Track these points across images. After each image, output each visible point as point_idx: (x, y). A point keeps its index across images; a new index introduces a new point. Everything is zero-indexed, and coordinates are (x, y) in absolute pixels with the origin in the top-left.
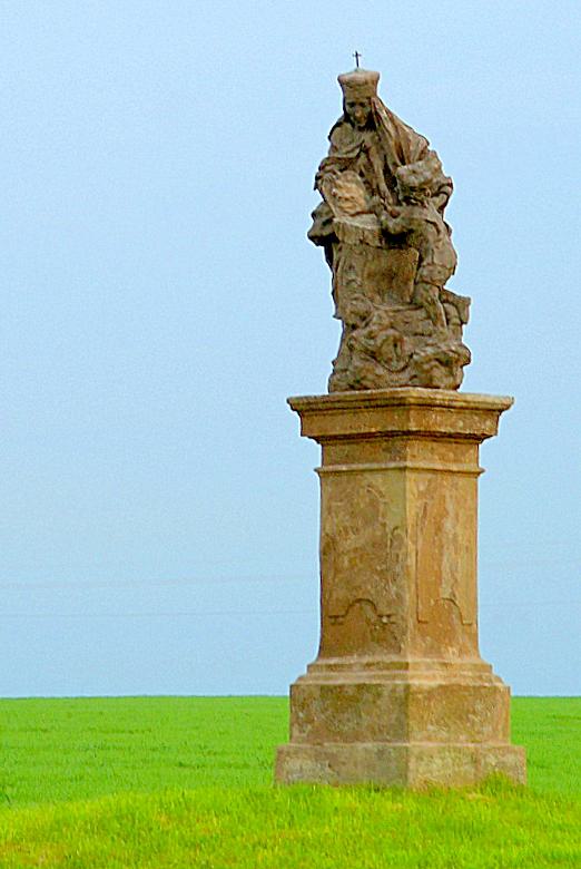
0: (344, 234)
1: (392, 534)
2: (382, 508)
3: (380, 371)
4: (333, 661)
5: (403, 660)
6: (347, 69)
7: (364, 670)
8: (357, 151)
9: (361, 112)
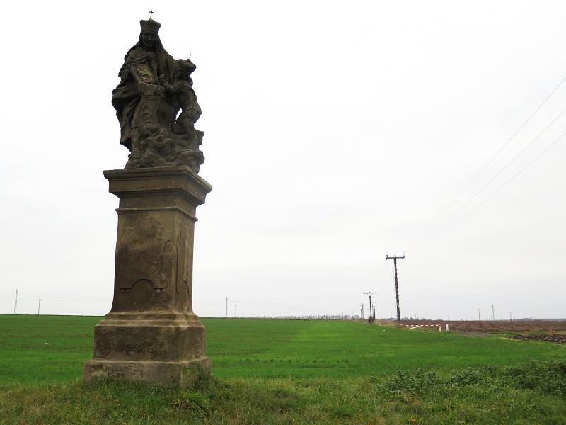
0: (145, 90)
1: (166, 244)
2: (159, 230)
3: (161, 159)
4: (123, 313)
5: (171, 313)
6: (147, 18)
7: (145, 319)
8: (144, 60)
9: (150, 30)
